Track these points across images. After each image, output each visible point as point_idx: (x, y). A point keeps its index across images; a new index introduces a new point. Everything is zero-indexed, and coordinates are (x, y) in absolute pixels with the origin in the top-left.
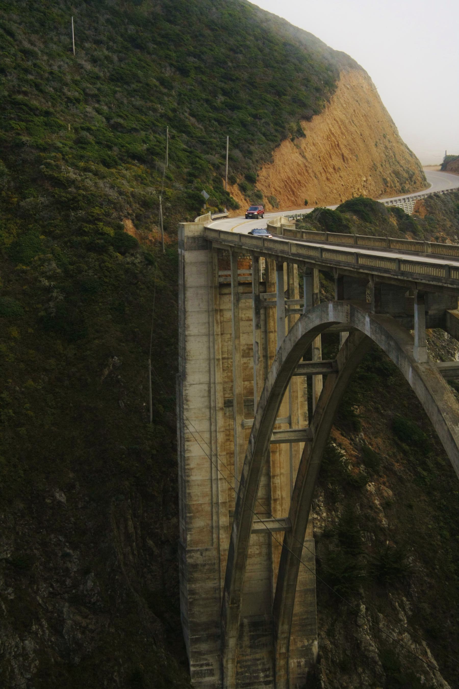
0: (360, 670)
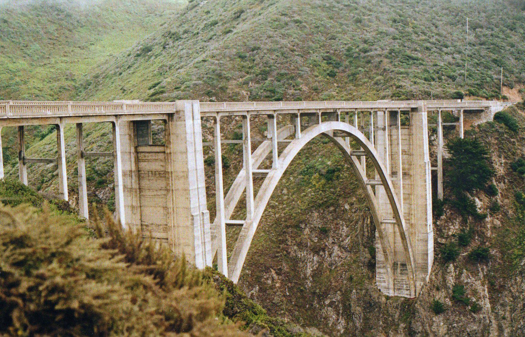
0: (443, 290)
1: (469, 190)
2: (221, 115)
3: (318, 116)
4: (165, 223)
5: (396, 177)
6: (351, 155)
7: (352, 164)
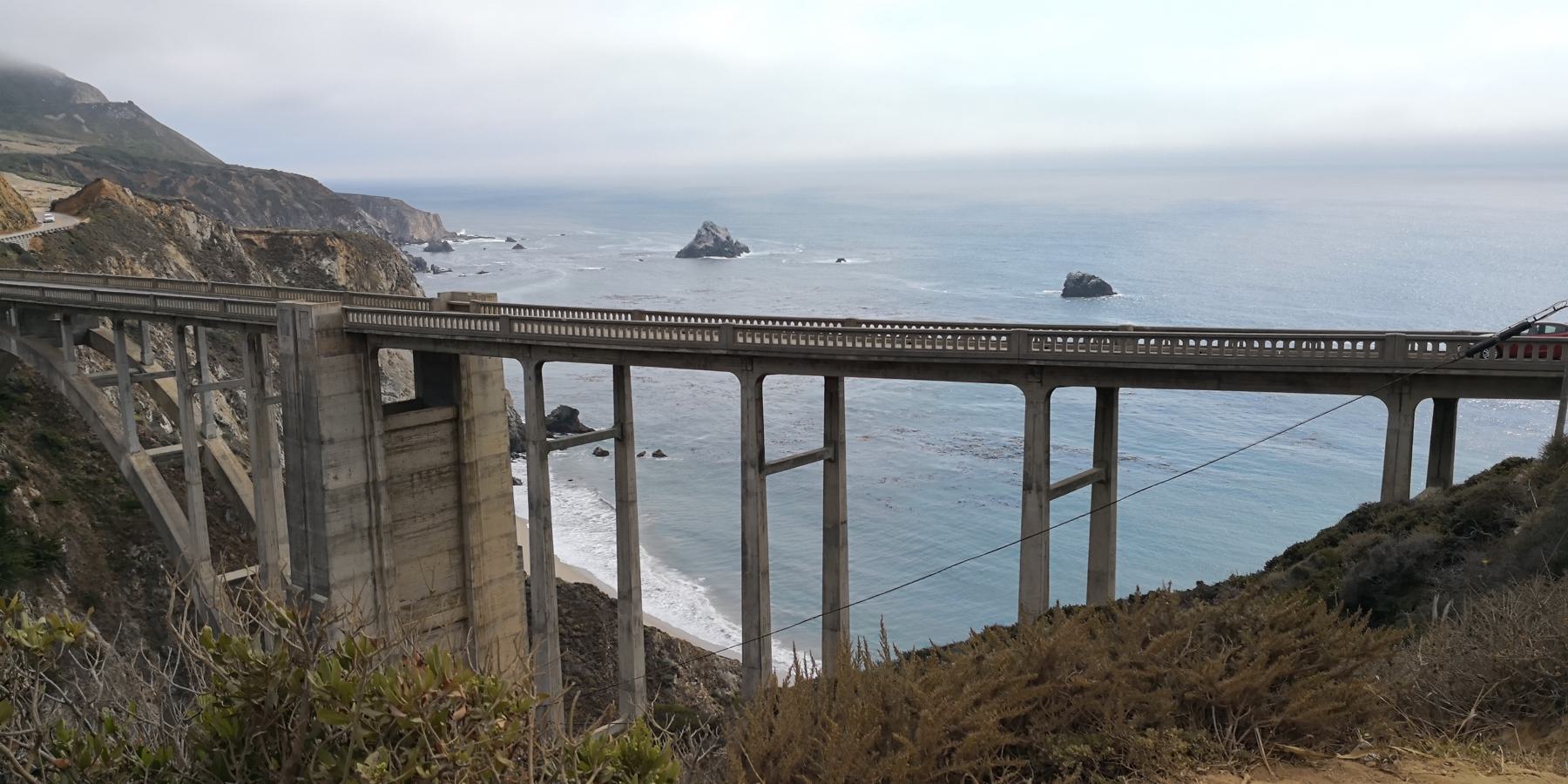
4: (454, 585)
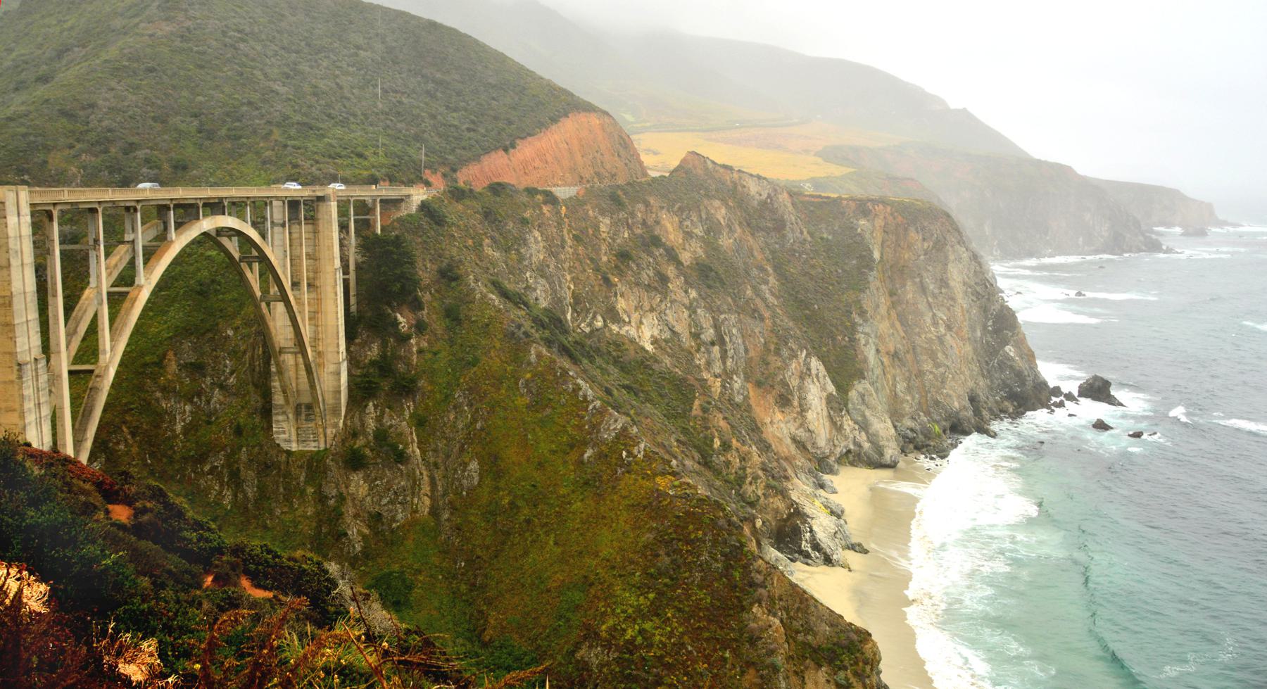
1: (389, 304)
2: (59, 207)
3: (198, 208)
5: (299, 290)
6: (241, 261)
7: (241, 274)
